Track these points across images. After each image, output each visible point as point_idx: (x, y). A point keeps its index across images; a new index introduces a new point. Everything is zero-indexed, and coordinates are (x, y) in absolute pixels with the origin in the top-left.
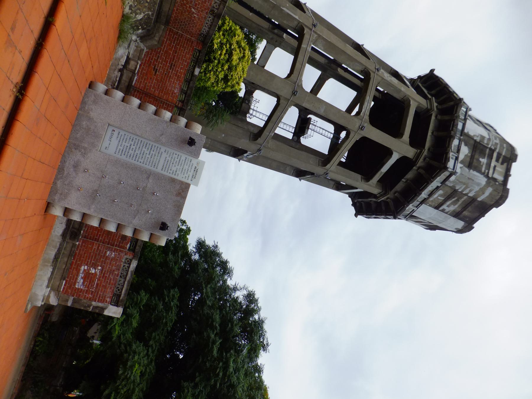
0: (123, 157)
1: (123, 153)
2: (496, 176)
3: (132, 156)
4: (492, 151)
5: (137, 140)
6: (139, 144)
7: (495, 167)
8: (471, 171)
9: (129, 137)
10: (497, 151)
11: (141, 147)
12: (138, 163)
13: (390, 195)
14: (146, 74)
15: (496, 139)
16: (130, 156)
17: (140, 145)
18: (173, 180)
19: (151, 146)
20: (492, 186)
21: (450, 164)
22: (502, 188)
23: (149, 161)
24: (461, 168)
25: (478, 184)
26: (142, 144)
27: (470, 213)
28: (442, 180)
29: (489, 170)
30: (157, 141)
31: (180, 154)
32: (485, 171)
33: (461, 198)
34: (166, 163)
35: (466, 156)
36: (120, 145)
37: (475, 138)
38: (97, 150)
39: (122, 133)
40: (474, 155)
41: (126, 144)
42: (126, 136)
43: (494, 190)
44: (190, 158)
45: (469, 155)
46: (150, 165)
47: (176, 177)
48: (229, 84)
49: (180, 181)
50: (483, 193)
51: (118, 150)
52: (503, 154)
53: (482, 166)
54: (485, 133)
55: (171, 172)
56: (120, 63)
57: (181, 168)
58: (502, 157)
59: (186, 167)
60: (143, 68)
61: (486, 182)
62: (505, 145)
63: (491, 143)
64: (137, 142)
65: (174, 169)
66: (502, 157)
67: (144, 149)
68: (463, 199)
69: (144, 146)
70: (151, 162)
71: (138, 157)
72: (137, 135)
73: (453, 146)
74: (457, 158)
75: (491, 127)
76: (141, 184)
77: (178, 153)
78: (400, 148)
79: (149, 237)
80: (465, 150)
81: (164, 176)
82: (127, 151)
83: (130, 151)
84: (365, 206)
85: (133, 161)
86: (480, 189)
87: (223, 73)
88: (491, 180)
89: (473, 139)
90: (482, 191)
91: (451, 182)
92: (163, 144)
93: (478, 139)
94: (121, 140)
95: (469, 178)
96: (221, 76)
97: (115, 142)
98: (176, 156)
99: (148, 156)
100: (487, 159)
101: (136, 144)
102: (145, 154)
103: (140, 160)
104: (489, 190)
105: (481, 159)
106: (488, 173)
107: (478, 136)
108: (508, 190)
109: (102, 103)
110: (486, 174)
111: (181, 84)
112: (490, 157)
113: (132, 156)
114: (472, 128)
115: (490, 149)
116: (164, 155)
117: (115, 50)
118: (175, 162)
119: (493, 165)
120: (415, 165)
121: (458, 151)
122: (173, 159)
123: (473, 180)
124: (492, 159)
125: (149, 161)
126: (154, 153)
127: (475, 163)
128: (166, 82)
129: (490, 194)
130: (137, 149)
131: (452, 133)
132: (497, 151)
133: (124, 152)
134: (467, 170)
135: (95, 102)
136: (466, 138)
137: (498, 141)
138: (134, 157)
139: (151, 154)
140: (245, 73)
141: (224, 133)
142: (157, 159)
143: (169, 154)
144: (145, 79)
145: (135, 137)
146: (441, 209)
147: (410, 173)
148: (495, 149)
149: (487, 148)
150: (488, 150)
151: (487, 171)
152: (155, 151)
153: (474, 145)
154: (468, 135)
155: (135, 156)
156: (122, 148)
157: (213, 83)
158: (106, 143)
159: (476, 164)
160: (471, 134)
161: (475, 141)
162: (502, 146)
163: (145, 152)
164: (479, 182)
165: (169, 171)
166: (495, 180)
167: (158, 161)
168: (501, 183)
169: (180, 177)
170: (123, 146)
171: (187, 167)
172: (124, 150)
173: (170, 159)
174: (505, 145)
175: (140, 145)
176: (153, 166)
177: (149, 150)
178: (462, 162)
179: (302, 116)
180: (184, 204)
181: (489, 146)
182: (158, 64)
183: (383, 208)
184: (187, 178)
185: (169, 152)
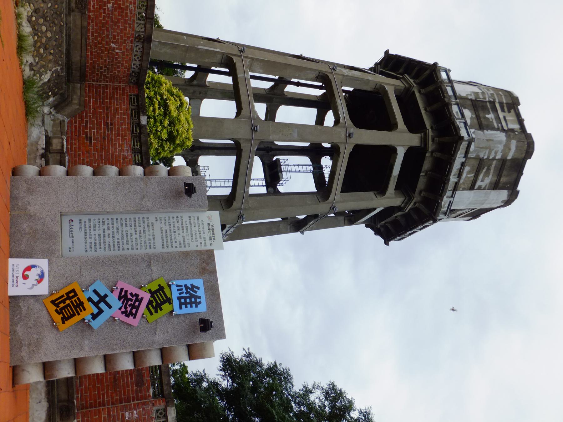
0: (101, 253)
1: (98, 247)
2: (511, 126)
3: (112, 246)
4: (493, 103)
5: (110, 220)
6: (115, 225)
7: (504, 117)
8: (485, 131)
9: (97, 221)
11: (120, 228)
12: (126, 252)
14: (79, 148)
15: (488, 90)
16: (109, 247)
17: (117, 226)
18: (187, 254)
19: (133, 220)
20: (513, 138)
21: (463, 133)
22: (523, 135)
23: (139, 242)
25: (500, 142)
26: (119, 223)
28: (463, 155)
29: (501, 123)
30: (140, 209)
31: (179, 215)
32: (498, 126)
34: (164, 237)
35: (471, 118)
36: (88, 236)
37: (470, 98)
38: (58, 257)
39: (85, 218)
41: (97, 232)
42: (92, 221)
43: (518, 141)
44: (196, 214)
45: (474, 116)
46: (144, 247)
47: (187, 249)
48: (177, 142)
49: (197, 251)
50: (510, 149)
51: (88, 245)
53: (492, 122)
54: (476, 89)
55: (178, 244)
56: (39, 147)
57: (189, 233)
58: (505, 105)
59: (195, 229)
60: (72, 143)
62: (500, 92)
63: (487, 96)
64: (110, 223)
65: (180, 239)
66: (505, 105)
67: (125, 229)
69: (124, 225)
70: (143, 242)
71: (121, 243)
72: (108, 213)
73: (454, 112)
74: (465, 124)
76: (143, 278)
77: (175, 215)
79: (187, 353)
80: (468, 113)
81: (170, 253)
82: (102, 241)
83: (107, 240)
85: (117, 253)
86: (505, 146)
87: (165, 131)
89: (468, 99)
90: (507, 147)
92: (149, 211)
93: (473, 97)
94: (88, 229)
95: (487, 140)
96: (164, 136)
97: (79, 235)
98: (175, 219)
99: (134, 236)
100: (493, 113)
101: (111, 226)
102: (129, 235)
103: (126, 247)
104: (514, 143)
105: (487, 116)
107: (471, 95)
108: (530, 134)
109: (41, 189)
110: (501, 128)
111: (129, 143)
112: (495, 110)
113: (112, 246)
115: (490, 102)
116: (157, 226)
117: (26, 134)
118: (176, 229)
119: (501, 116)
121: (463, 116)
122: (172, 226)
123: (493, 140)
124: (497, 111)
125: (139, 242)
126: (141, 228)
127: (484, 122)
128: (109, 148)
129: (517, 147)
130: (115, 233)
132: (497, 101)
133: (98, 245)
134: (480, 132)
135: (30, 191)
136: (461, 101)
138: (116, 246)
139: (138, 233)
140: (191, 122)
142: (149, 235)
143: (163, 222)
144: (80, 155)
145: (106, 217)
148: (494, 99)
149: (486, 102)
150: (488, 104)
151: (500, 125)
152: (142, 225)
154: (461, 98)
155: (116, 243)
156: (93, 241)
157: (157, 149)
158: (67, 242)
159: (486, 123)
160: (463, 94)
161: (471, 100)
163: (129, 232)
164: (499, 139)
165: (174, 245)
166: (512, 130)
167: (152, 237)
168: (520, 131)
169: (194, 246)
170: (93, 236)
171: (197, 229)
172: (98, 242)
173: (167, 227)
174: (500, 92)
175: (117, 226)
176: (148, 247)
177: (133, 227)
180: (217, 281)
182: (90, 130)
184: (203, 244)
185: (163, 219)
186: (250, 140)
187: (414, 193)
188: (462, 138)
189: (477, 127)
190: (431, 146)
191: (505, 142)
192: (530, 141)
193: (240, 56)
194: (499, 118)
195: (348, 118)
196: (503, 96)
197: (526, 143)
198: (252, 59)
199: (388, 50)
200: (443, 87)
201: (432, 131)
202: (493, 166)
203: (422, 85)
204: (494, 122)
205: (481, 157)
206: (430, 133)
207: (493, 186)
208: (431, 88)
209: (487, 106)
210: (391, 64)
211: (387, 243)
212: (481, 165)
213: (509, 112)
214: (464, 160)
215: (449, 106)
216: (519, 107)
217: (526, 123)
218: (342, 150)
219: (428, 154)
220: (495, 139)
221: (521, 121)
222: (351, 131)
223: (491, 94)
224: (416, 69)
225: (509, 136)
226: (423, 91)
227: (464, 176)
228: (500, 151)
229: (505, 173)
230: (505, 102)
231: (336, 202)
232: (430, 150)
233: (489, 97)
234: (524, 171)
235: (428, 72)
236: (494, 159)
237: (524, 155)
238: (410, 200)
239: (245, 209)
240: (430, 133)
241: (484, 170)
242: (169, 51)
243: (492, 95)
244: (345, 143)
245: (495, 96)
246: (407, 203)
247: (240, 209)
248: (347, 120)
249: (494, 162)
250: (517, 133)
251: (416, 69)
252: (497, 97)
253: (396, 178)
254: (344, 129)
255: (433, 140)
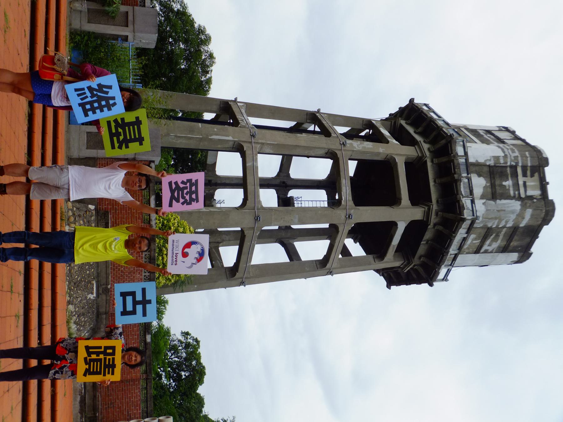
2: (530, 193)
4: (514, 168)
7: (525, 183)
8: (498, 201)
10: (520, 164)
13: (416, 261)
15: (513, 151)
21: (467, 214)
22: (543, 203)
24: (483, 204)
25: (513, 212)
27: (520, 243)
29: (519, 190)
32: (514, 193)
33: (500, 232)
35: (485, 187)
37: (488, 164)
40: (495, 182)
43: (535, 210)
45: (488, 184)
50: (523, 218)
52: (529, 165)
53: (509, 189)
58: (529, 168)
61: (521, 205)
63: (509, 160)
66: (529, 168)
68: (503, 233)
75: (507, 129)
78: (403, 215)
80: (479, 183)
84: (394, 278)
86: (517, 215)
88: (526, 200)
90: (521, 216)
91: (479, 223)
93: (492, 163)
95: (498, 211)
104: (529, 213)
105: (504, 183)
106: (519, 194)
107: (490, 160)
110: (517, 196)
112: (515, 175)
114: (480, 152)
115: (511, 166)
119: (521, 183)
120: (428, 225)
123: (504, 210)
124: (517, 176)
127: (499, 190)
129: (532, 216)
131: (456, 176)
132: (520, 164)
134: (492, 202)
136: (477, 168)
137: (517, 154)
141: (195, 285)
146: (482, 250)
147: (427, 233)
149: (506, 167)
150: (508, 169)
151: (517, 193)
153: (490, 171)
159: (501, 192)
160: (481, 160)
161: (489, 166)
162: (523, 156)
166: (531, 198)
168: (540, 197)
178: (482, 197)
179: (281, 196)
181: (509, 164)
183: (415, 276)
186: (253, 228)
187: (414, 258)
188: (464, 220)
189: (490, 196)
190: (433, 219)
191: (518, 211)
192: (551, 208)
193: (251, 143)
194: (518, 184)
195: (351, 198)
196: (529, 159)
197: (544, 211)
198: (263, 144)
199: (413, 99)
200: (455, 161)
201: (438, 206)
202: (503, 233)
203: (436, 154)
204: (511, 189)
205: (489, 226)
206: (435, 207)
207: (501, 249)
208: (444, 159)
209: (506, 171)
210: (414, 120)
211: (389, 286)
212: (488, 233)
213: (532, 176)
214: (466, 235)
215: (458, 183)
216: (546, 169)
217: (549, 187)
218: (341, 229)
219: (429, 227)
220: (507, 209)
221: (543, 185)
222: (352, 212)
223: (515, 157)
224: (434, 133)
225: (526, 203)
226: (436, 161)
227: (469, 241)
228: (512, 220)
229: (516, 237)
230: (529, 165)
231: (333, 269)
232: (432, 224)
233: (511, 161)
234: (540, 235)
235: (443, 142)
236: (504, 227)
237: (540, 222)
238: (409, 264)
239: (245, 278)
240: (435, 207)
241: (492, 237)
242: (184, 141)
243: (516, 157)
244: (344, 224)
245: (520, 159)
246: (406, 266)
247: (242, 278)
248: (349, 200)
249: (504, 230)
250: (535, 200)
251: (434, 133)
252: (522, 159)
253: (396, 247)
254: (345, 211)
255: (437, 214)
